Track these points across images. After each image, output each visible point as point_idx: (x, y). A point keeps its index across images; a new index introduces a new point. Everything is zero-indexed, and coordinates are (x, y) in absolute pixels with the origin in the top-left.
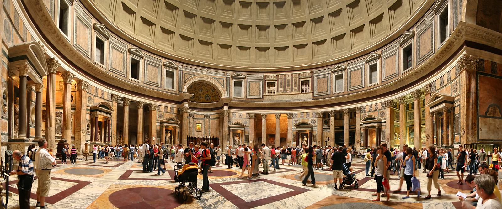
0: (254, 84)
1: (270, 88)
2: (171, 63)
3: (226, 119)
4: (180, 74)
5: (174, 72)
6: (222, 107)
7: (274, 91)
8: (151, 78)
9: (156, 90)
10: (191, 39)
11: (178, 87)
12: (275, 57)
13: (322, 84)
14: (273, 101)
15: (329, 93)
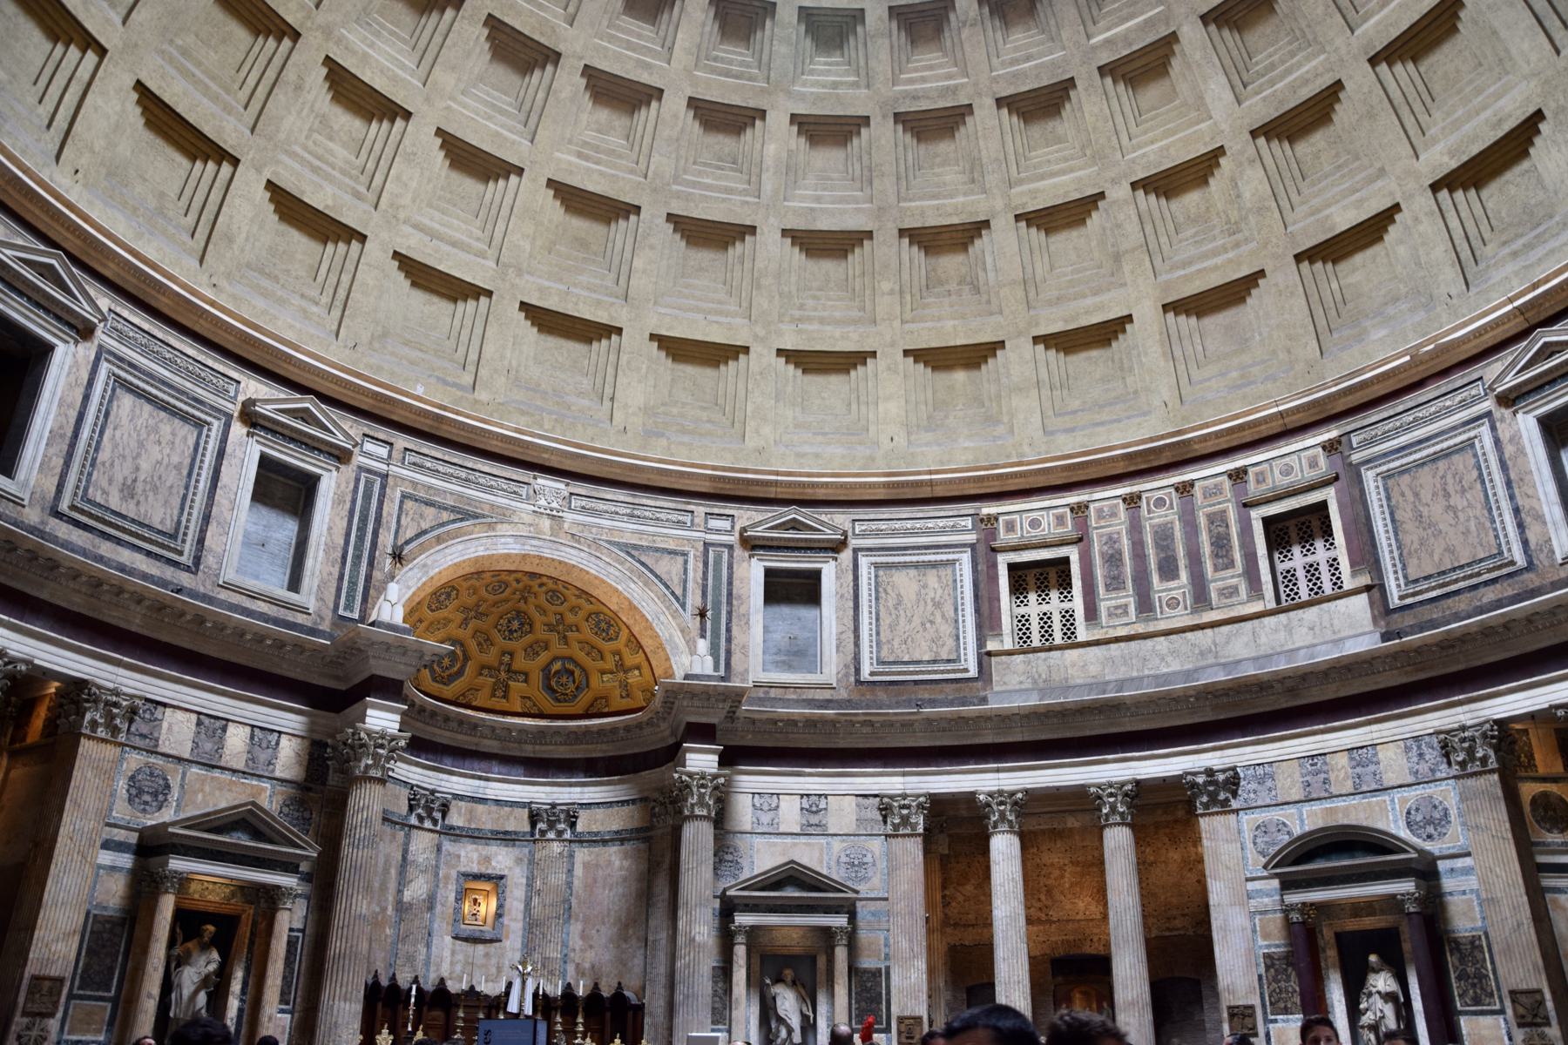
0: (905, 583)
1: (1032, 597)
2: (305, 416)
3: (697, 837)
4: (367, 497)
5: (317, 478)
6: (672, 754)
7: (1068, 616)
8: (128, 491)
9: (145, 576)
10: (477, 292)
11: (334, 584)
12: (1046, 392)
13: (1436, 510)
14: (1068, 688)
15: (1521, 561)
